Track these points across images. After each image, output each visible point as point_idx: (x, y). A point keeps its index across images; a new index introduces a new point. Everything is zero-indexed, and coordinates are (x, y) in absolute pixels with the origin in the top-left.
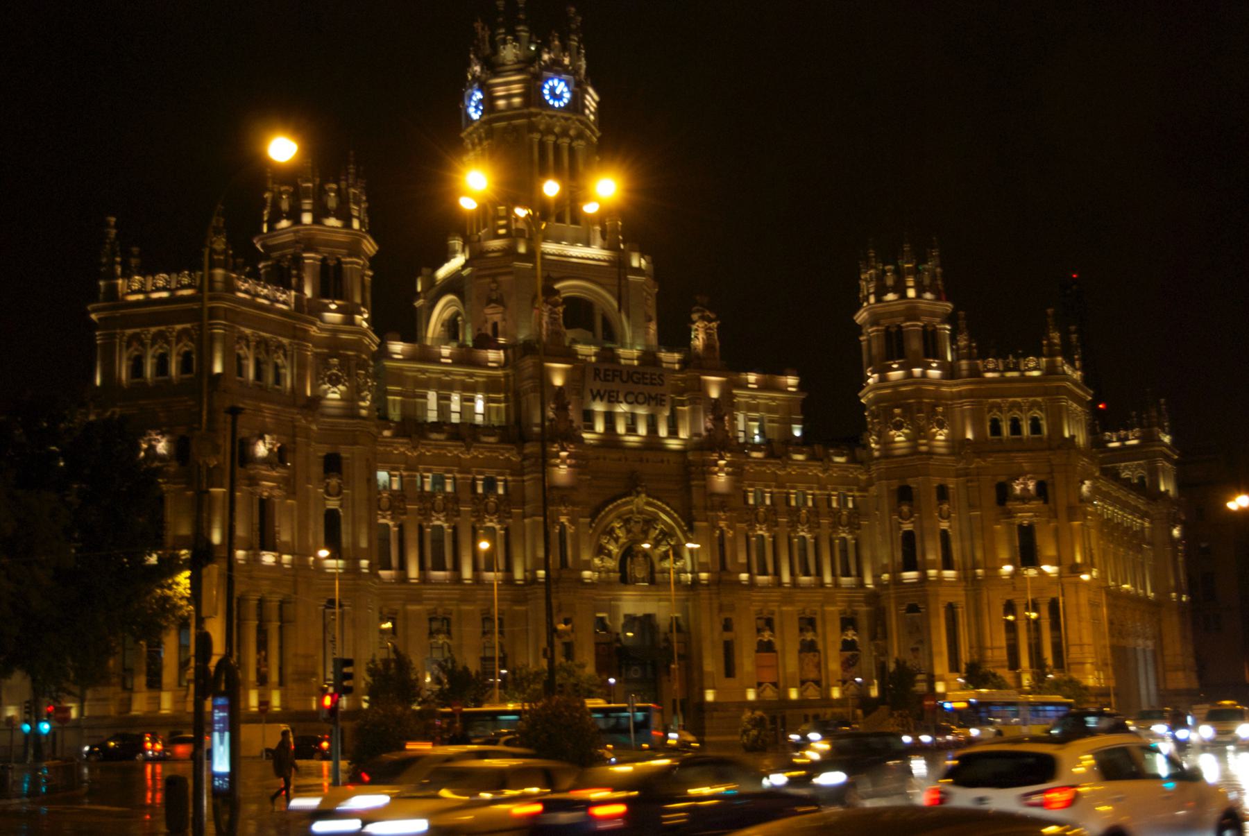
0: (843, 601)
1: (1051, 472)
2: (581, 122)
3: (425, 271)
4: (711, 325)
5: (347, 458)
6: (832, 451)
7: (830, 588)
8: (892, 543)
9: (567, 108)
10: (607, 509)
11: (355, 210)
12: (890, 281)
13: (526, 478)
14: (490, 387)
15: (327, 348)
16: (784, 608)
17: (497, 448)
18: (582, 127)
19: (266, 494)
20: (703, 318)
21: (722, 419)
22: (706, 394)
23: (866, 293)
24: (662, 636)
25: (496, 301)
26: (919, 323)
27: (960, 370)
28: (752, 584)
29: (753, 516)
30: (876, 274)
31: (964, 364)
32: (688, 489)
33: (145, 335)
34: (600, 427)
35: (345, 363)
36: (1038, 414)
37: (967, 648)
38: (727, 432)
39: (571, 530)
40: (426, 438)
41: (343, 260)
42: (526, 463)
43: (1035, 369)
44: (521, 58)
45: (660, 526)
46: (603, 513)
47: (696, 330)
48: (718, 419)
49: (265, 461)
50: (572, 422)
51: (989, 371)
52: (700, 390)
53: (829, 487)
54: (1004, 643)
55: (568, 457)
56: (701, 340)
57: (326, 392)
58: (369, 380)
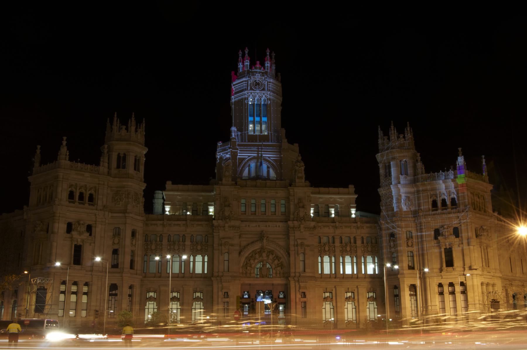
4: (301, 168)
29: (323, 248)
32: (289, 238)
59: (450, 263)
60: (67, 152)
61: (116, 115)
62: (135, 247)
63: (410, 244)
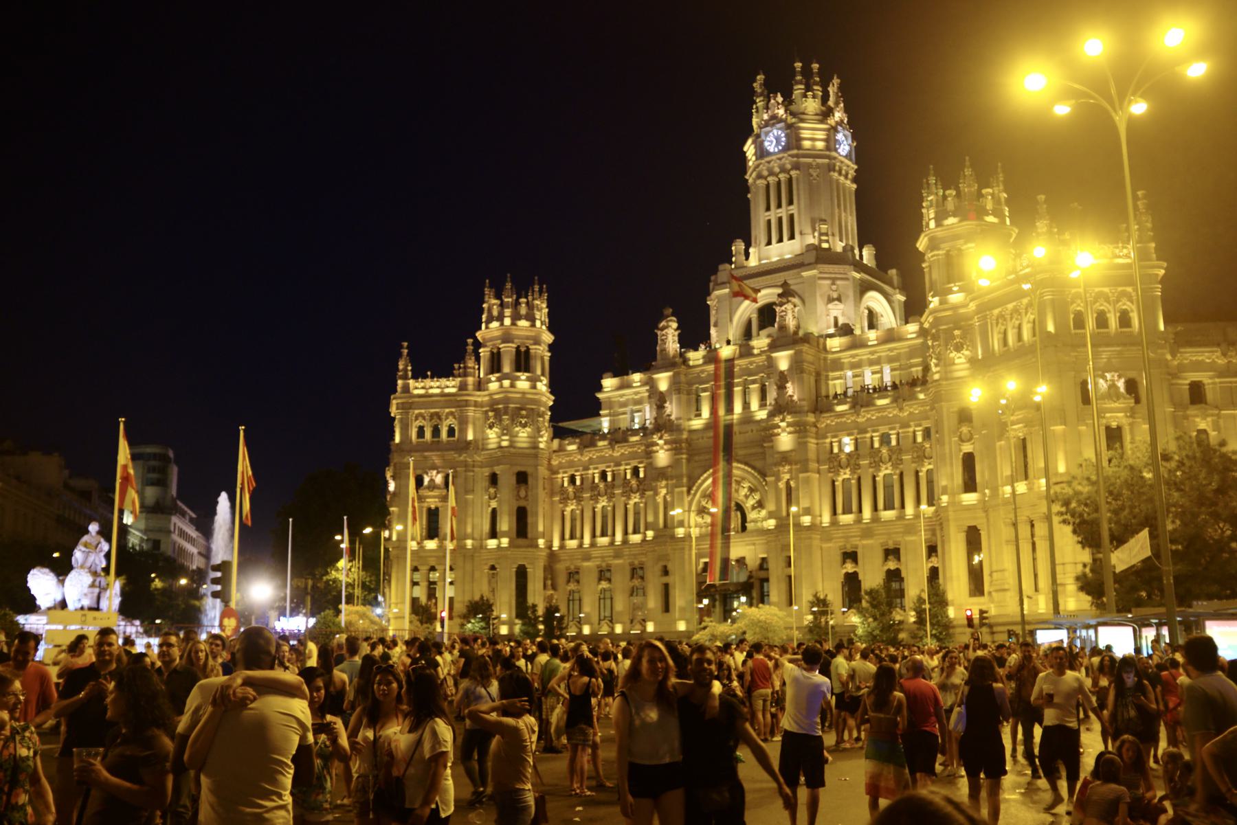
4: (783, 308)
18: (795, 159)
29: (836, 464)
34: (706, 412)
35: (498, 414)
38: (791, 396)
40: (595, 445)
45: (746, 485)
50: (669, 415)
52: (772, 367)
53: (912, 423)
55: (665, 444)
62: (527, 500)
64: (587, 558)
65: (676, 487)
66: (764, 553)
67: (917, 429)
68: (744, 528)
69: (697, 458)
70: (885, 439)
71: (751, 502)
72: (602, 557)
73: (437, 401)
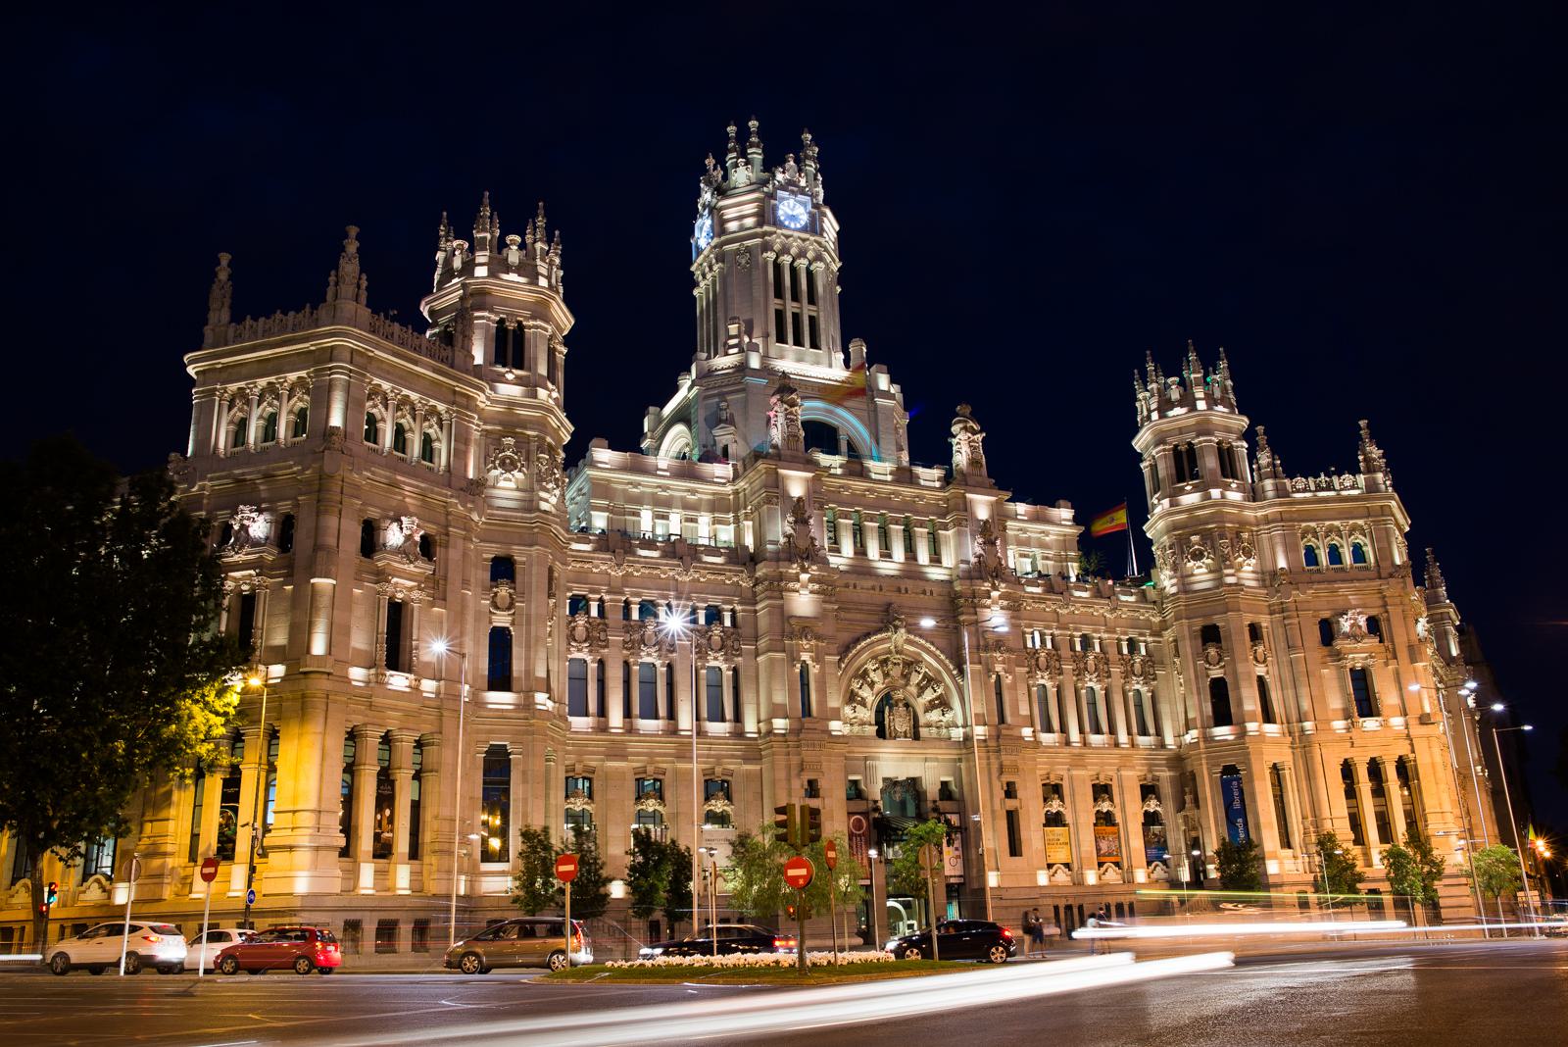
0: (1142, 765)
1: (1385, 605)
2: (819, 244)
3: (652, 409)
4: (976, 437)
5: (524, 563)
6: (1118, 589)
7: (1127, 749)
8: (1199, 694)
9: (804, 229)
10: (859, 647)
11: (543, 269)
12: (1175, 394)
13: (758, 607)
14: (718, 506)
15: (500, 424)
16: (1074, 772)
17: (725, 570)
19: (400, 595)
20: (965, 429)
21: (993, 544)
22: (973, 515)
23: (1145, 413)
24: (930, 805)
25: (726, 421)
26: (1213, 438)
27: (1264, 491)
28: (1037, 743)
29: (1033, 662)
30: (1158, 389)
31: (1269, 484)
33: (251, 389)
36: (1360, 539)
37: (1300, 817)
39: (814, 670)
41: (524, 323)
42: (759, 588)
43: (1353, 487)
44: (753, 180)
46: (854, 651)
47: (958, 443)
48: (990, 543)
49: (399, 551)
51: (1298, 491)
52: (966, 510)
54: (1345, 813)
55: (811, 580)
56: (964, 454)
57: (497, 478)
58: (556, 471)
59: (1365, 703)
60: (360, 279)
61: (486, 201)
63: (1261, 658)
64: (617, 752)
65: (827, 654)
66: (949, 775)
67: (1122, 637)
68: (916, 737)
69: (842, 615)
70: (1086, 642)
71: (929, 695)
72: (651, 755)
73: (418, 375)
